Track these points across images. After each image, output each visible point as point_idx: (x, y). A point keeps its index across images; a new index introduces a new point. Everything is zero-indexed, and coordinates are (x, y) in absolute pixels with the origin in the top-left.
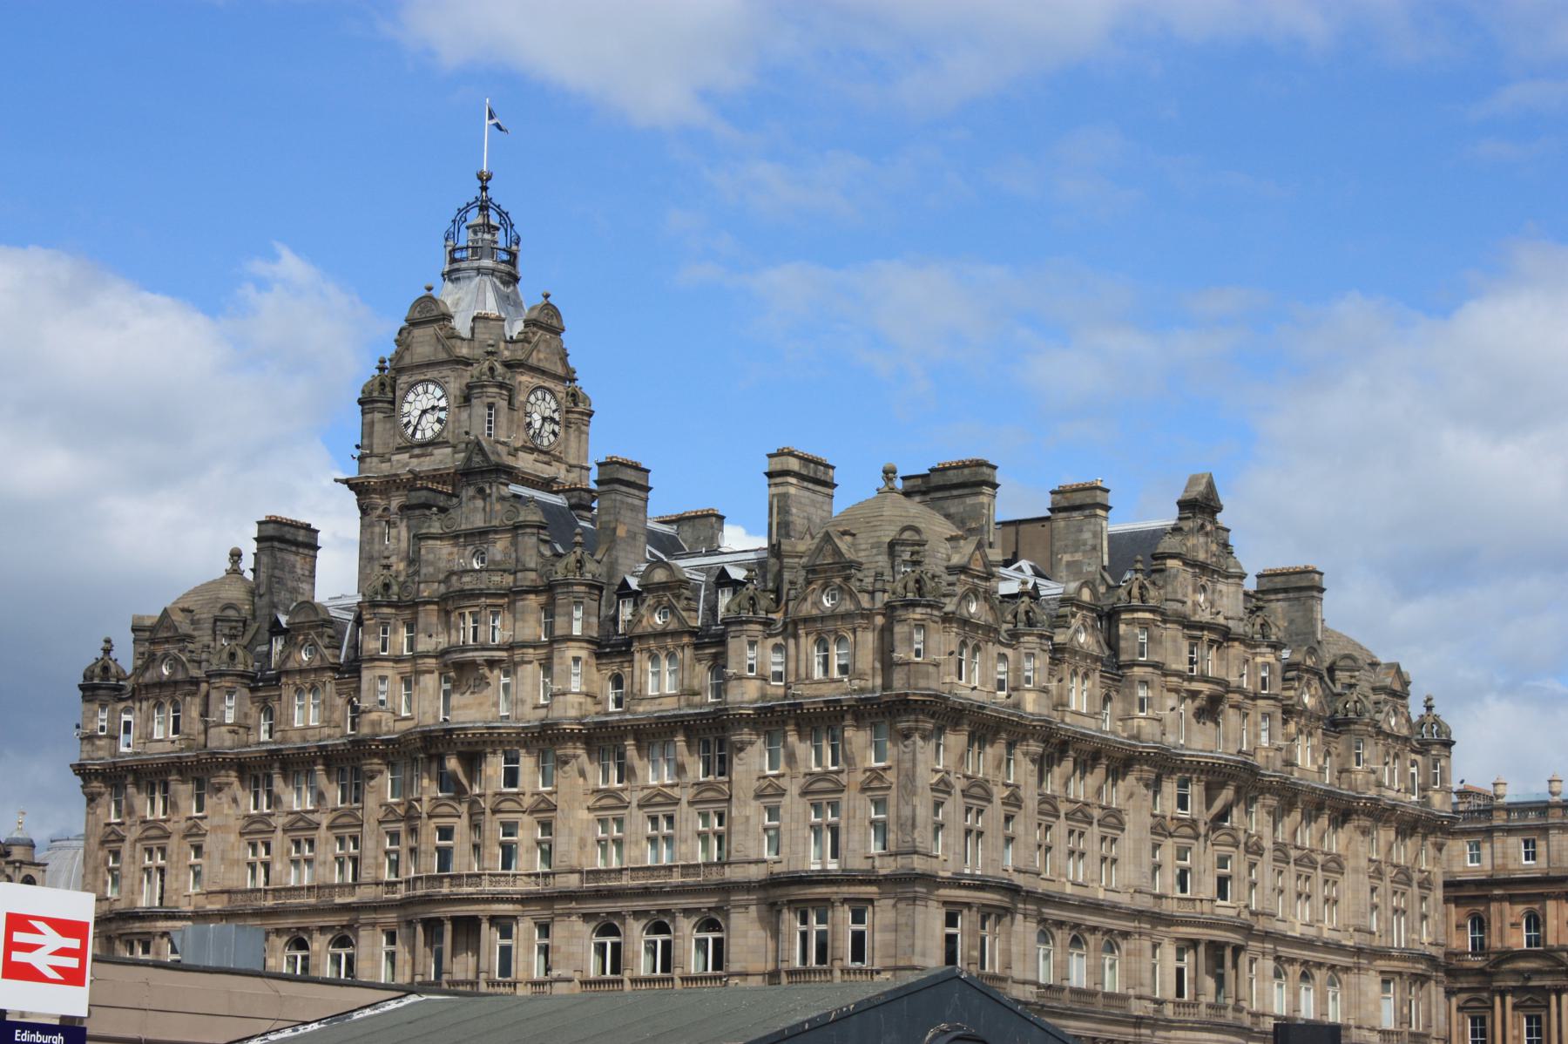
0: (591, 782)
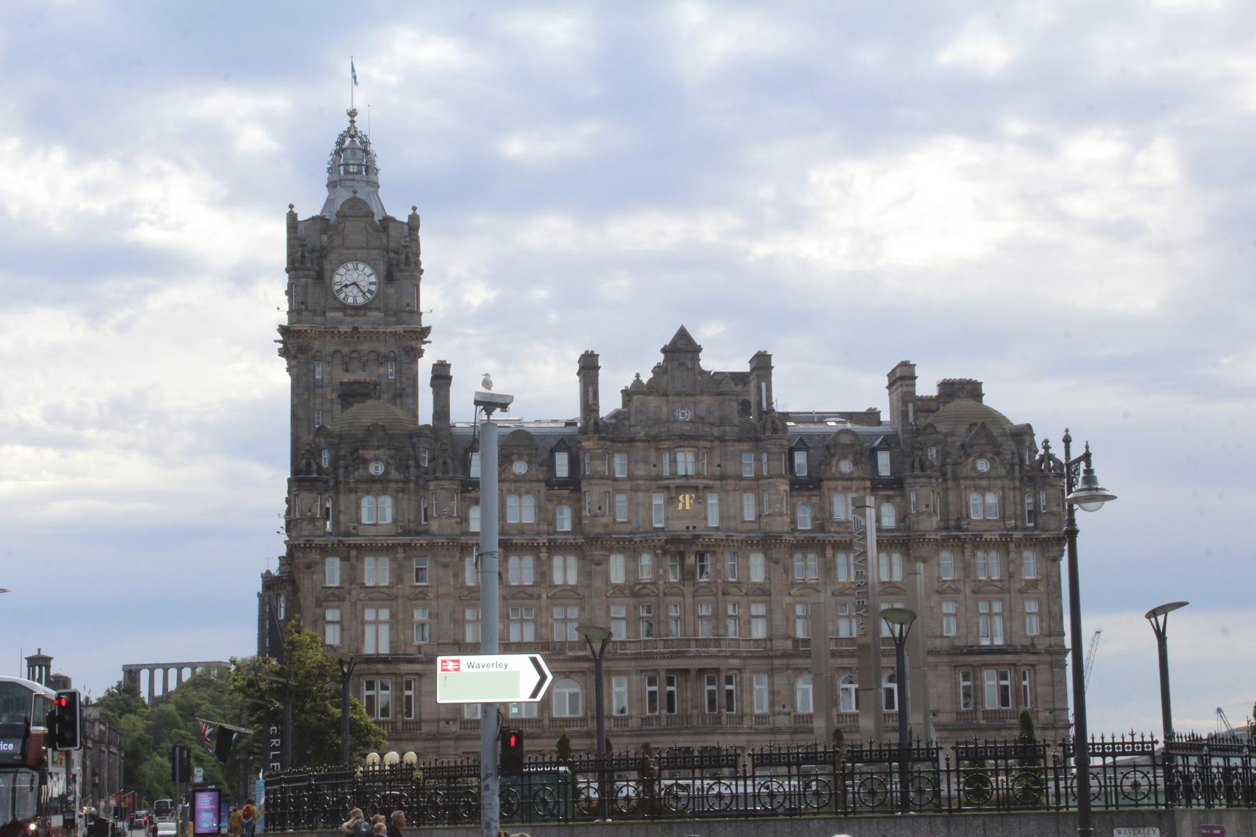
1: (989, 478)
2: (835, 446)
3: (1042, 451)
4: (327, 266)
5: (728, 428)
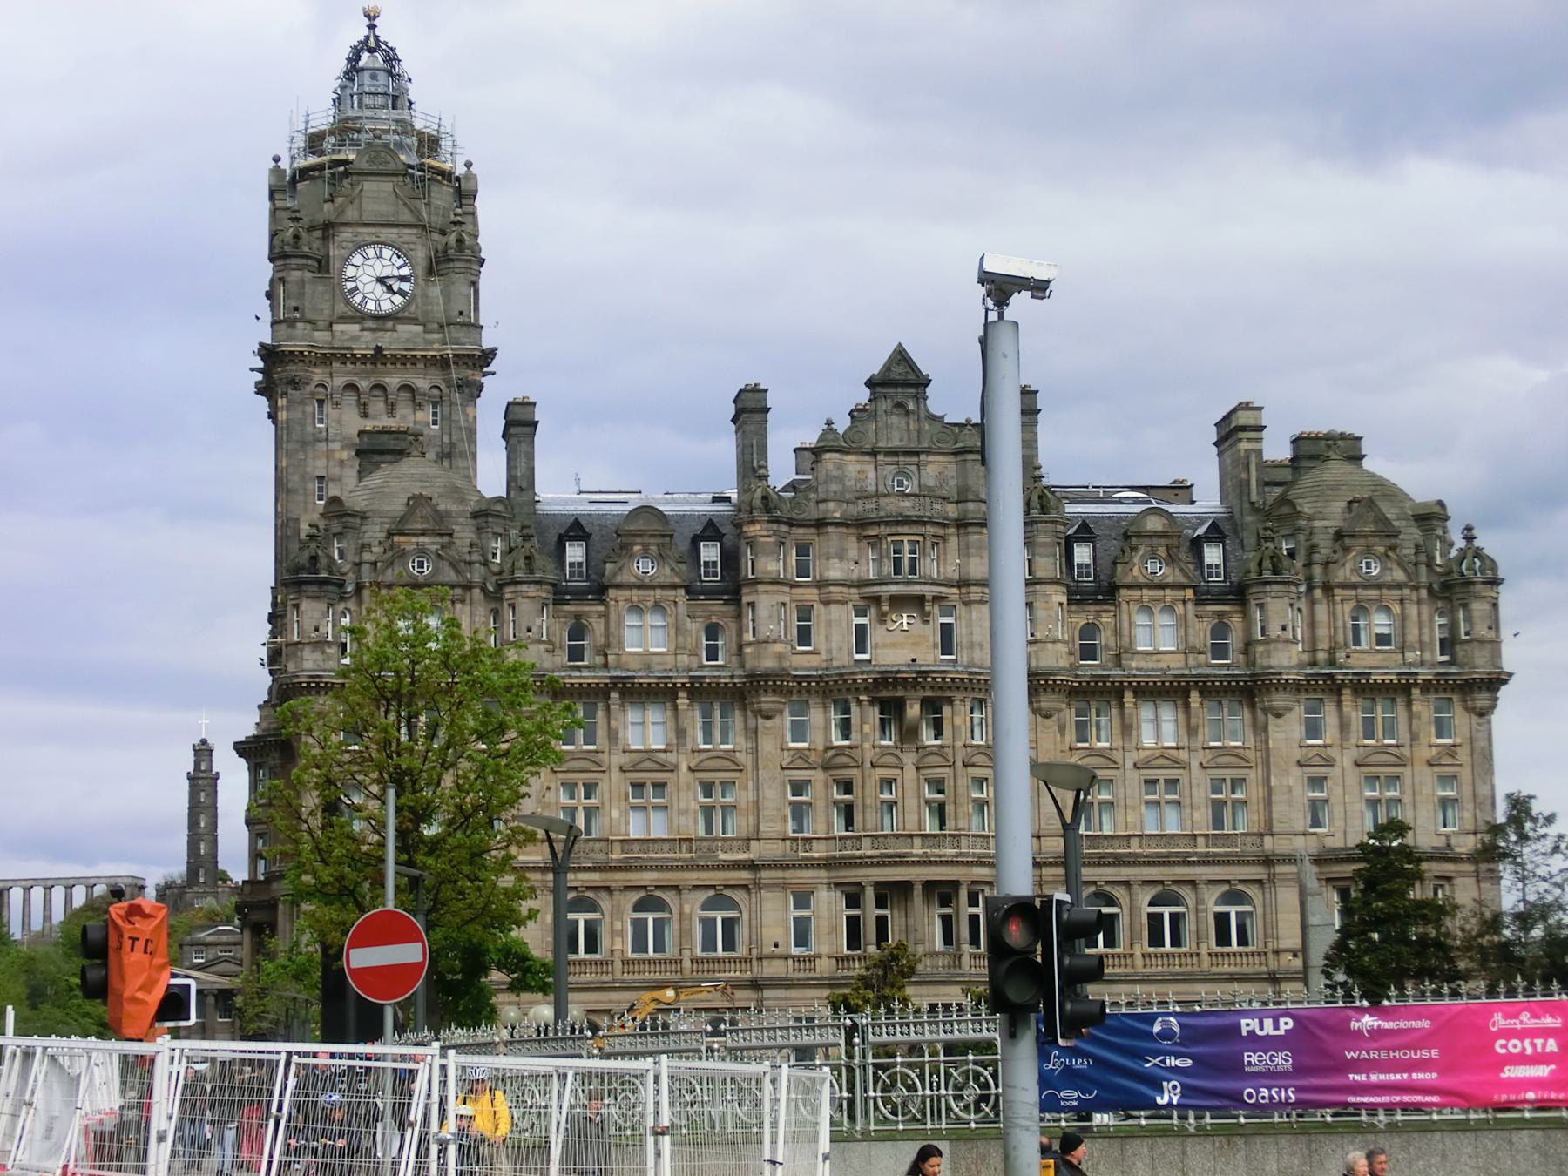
0: (1068, 738)
1: (1379, 586)
2: (1139, 535)
3: (1460, 543)
4: (334, 252)
5: (971, 506)
